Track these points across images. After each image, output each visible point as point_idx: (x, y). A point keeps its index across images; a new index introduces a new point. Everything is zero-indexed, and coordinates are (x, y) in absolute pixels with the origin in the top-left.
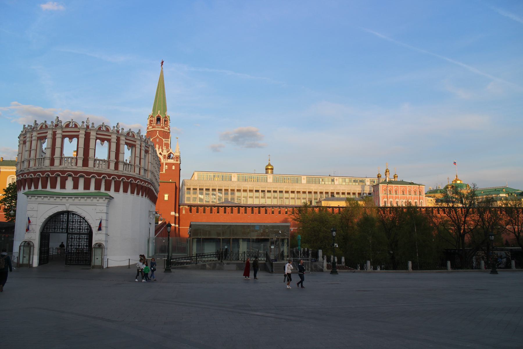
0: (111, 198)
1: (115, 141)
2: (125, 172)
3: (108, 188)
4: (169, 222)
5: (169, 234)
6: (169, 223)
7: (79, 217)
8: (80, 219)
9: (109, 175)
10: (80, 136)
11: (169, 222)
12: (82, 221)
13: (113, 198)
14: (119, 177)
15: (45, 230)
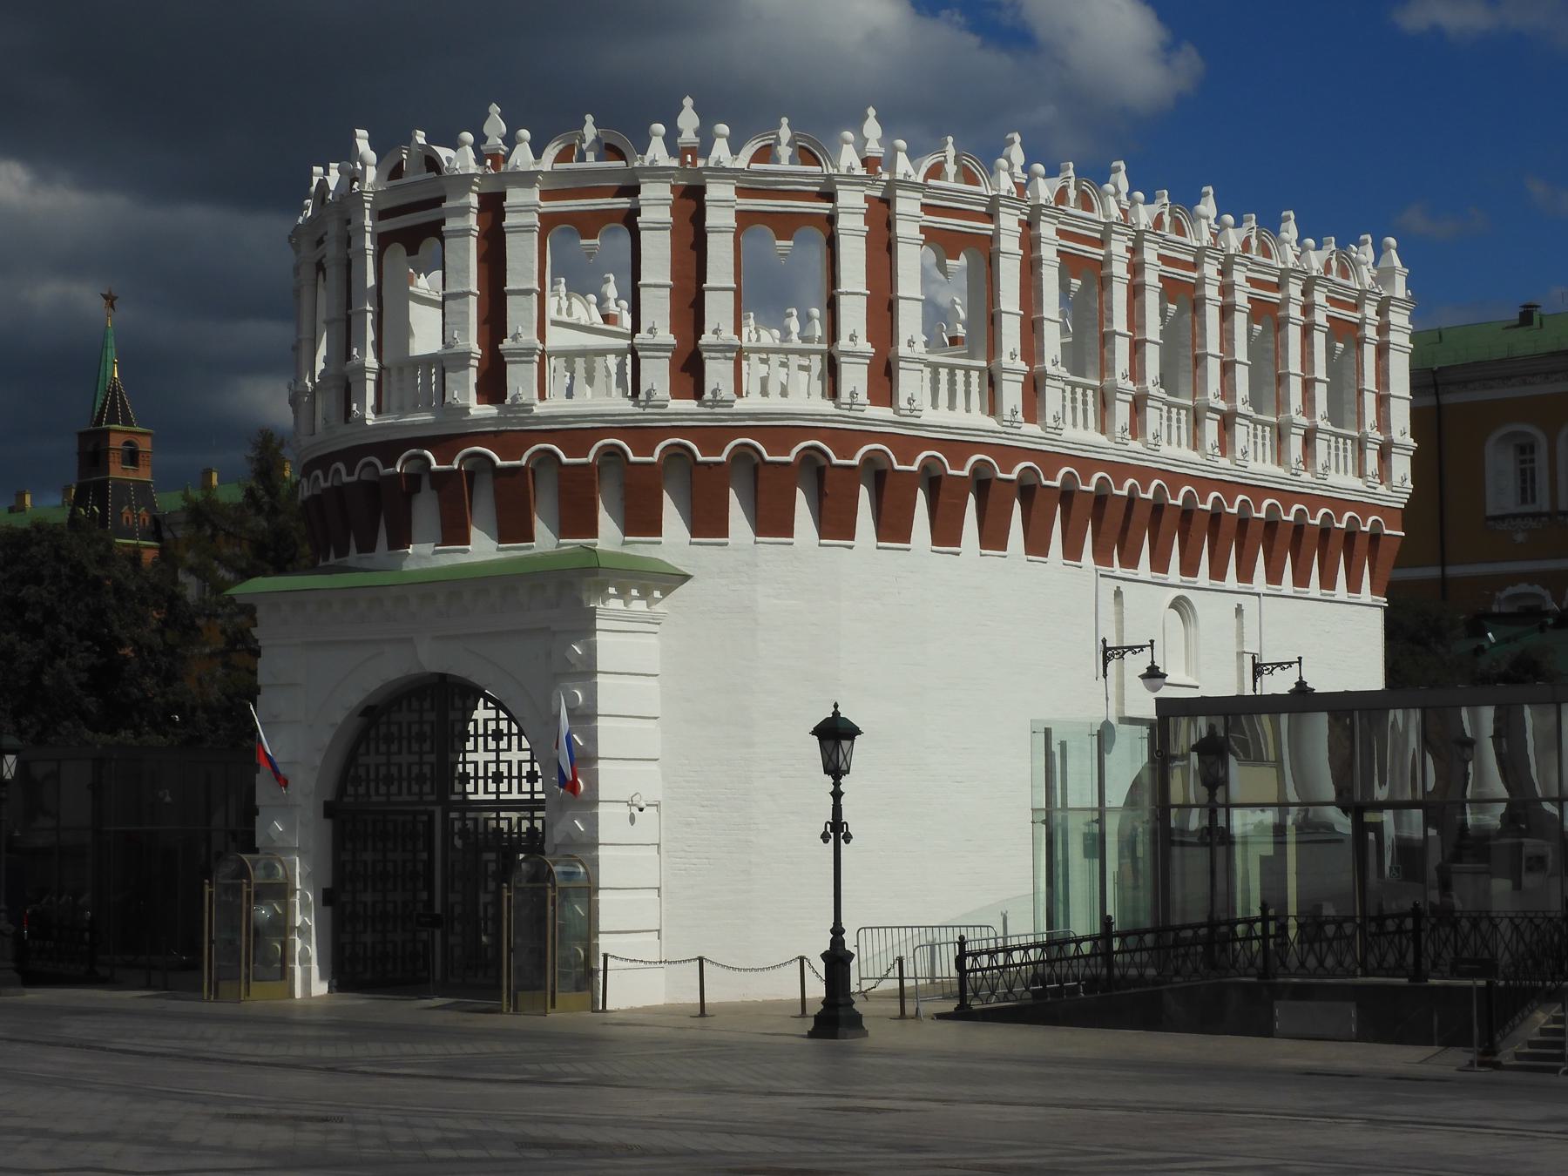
0: (672, 579)
1: (664, 215)
2: (740, 405)
3: (644, 522)
4: (836, 706)
5: (837, 784)
6: (836, 714)
7: (490, 705)
8: (498, 719)
9: (643, 435)
10: (451, 224)
11: (836, 706)
12: (504, 725)
13: (686, 578)
14: (712, 436)
15: (350, 790)
